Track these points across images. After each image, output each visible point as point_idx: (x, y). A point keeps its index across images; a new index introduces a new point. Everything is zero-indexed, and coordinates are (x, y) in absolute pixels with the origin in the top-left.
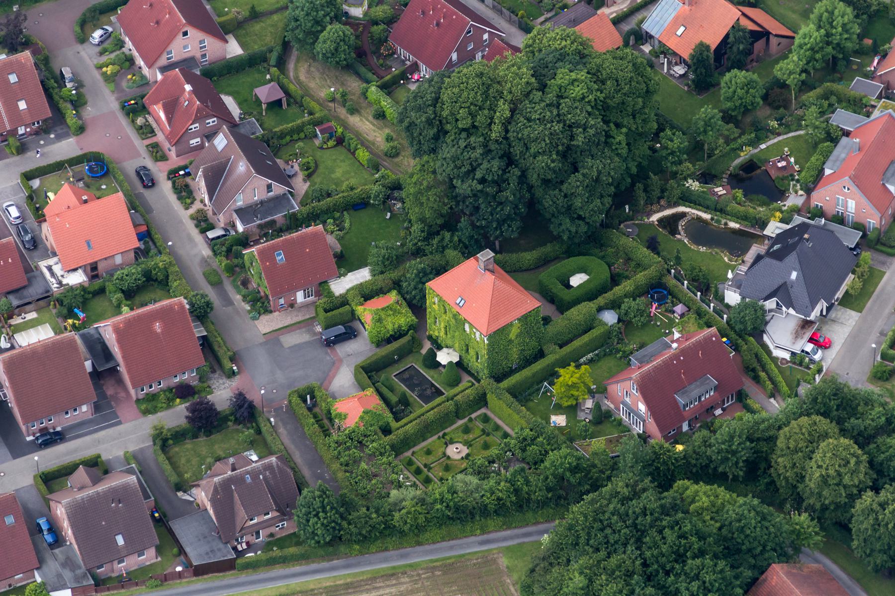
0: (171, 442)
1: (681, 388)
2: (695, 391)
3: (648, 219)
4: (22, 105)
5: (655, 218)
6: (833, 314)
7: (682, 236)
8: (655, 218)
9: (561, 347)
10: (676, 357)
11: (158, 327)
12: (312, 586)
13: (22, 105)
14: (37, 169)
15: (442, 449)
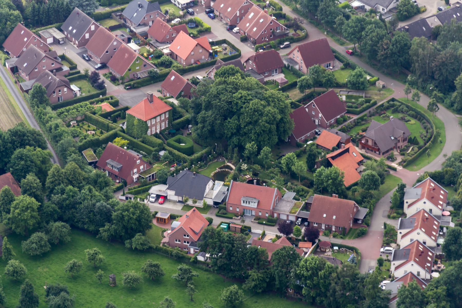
0: (88, 79)
1: (114, 159)
2: (114, 163)
3: (228, 162)
4: (255, 29)
5: (228, 164)
6: (179, 204)
7: (218, 170)
8: (228, 164)
9: (143, 142)
10: (123, 151)
11: (127, 55)
12: (17, 110)
13: (255, 29)
14: (228, 42)
15: (90, 129)
